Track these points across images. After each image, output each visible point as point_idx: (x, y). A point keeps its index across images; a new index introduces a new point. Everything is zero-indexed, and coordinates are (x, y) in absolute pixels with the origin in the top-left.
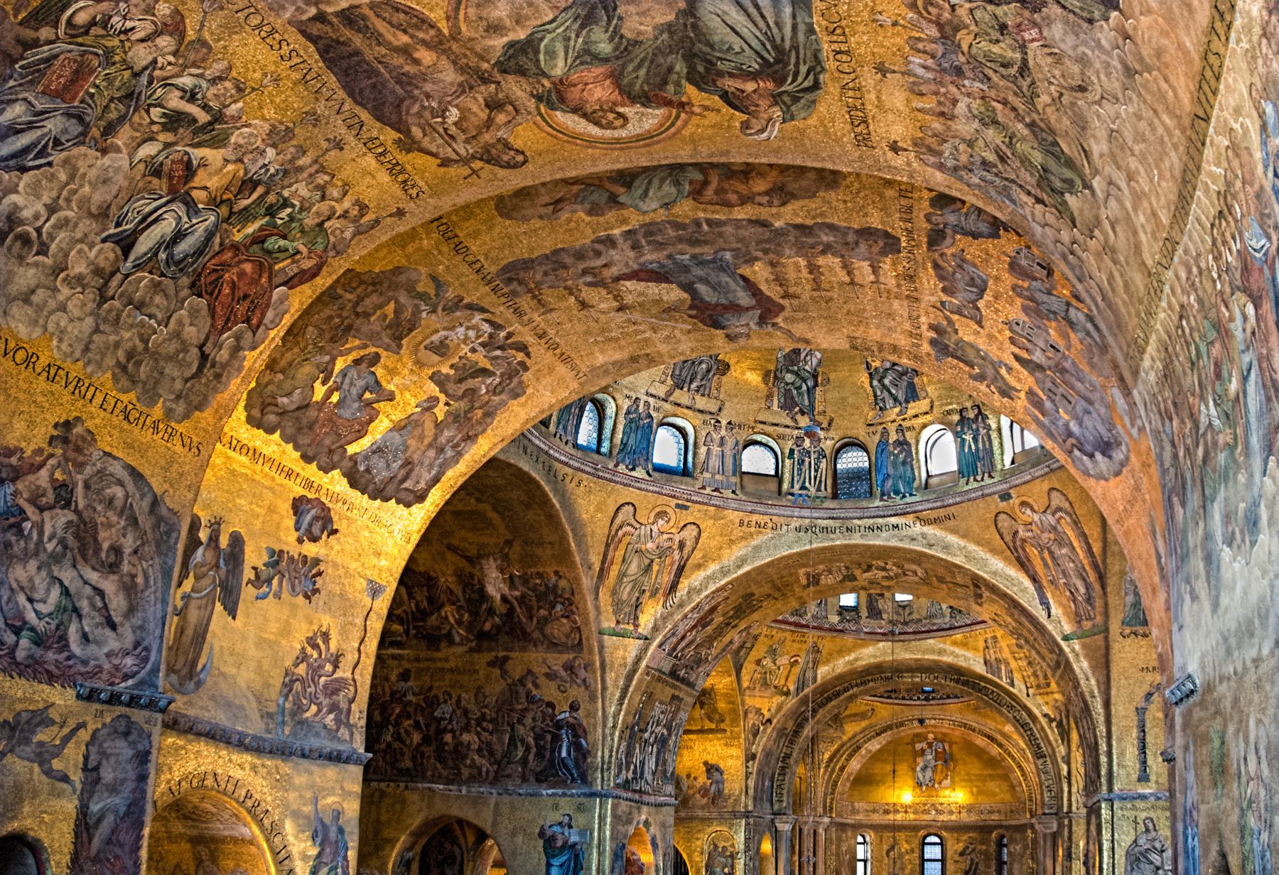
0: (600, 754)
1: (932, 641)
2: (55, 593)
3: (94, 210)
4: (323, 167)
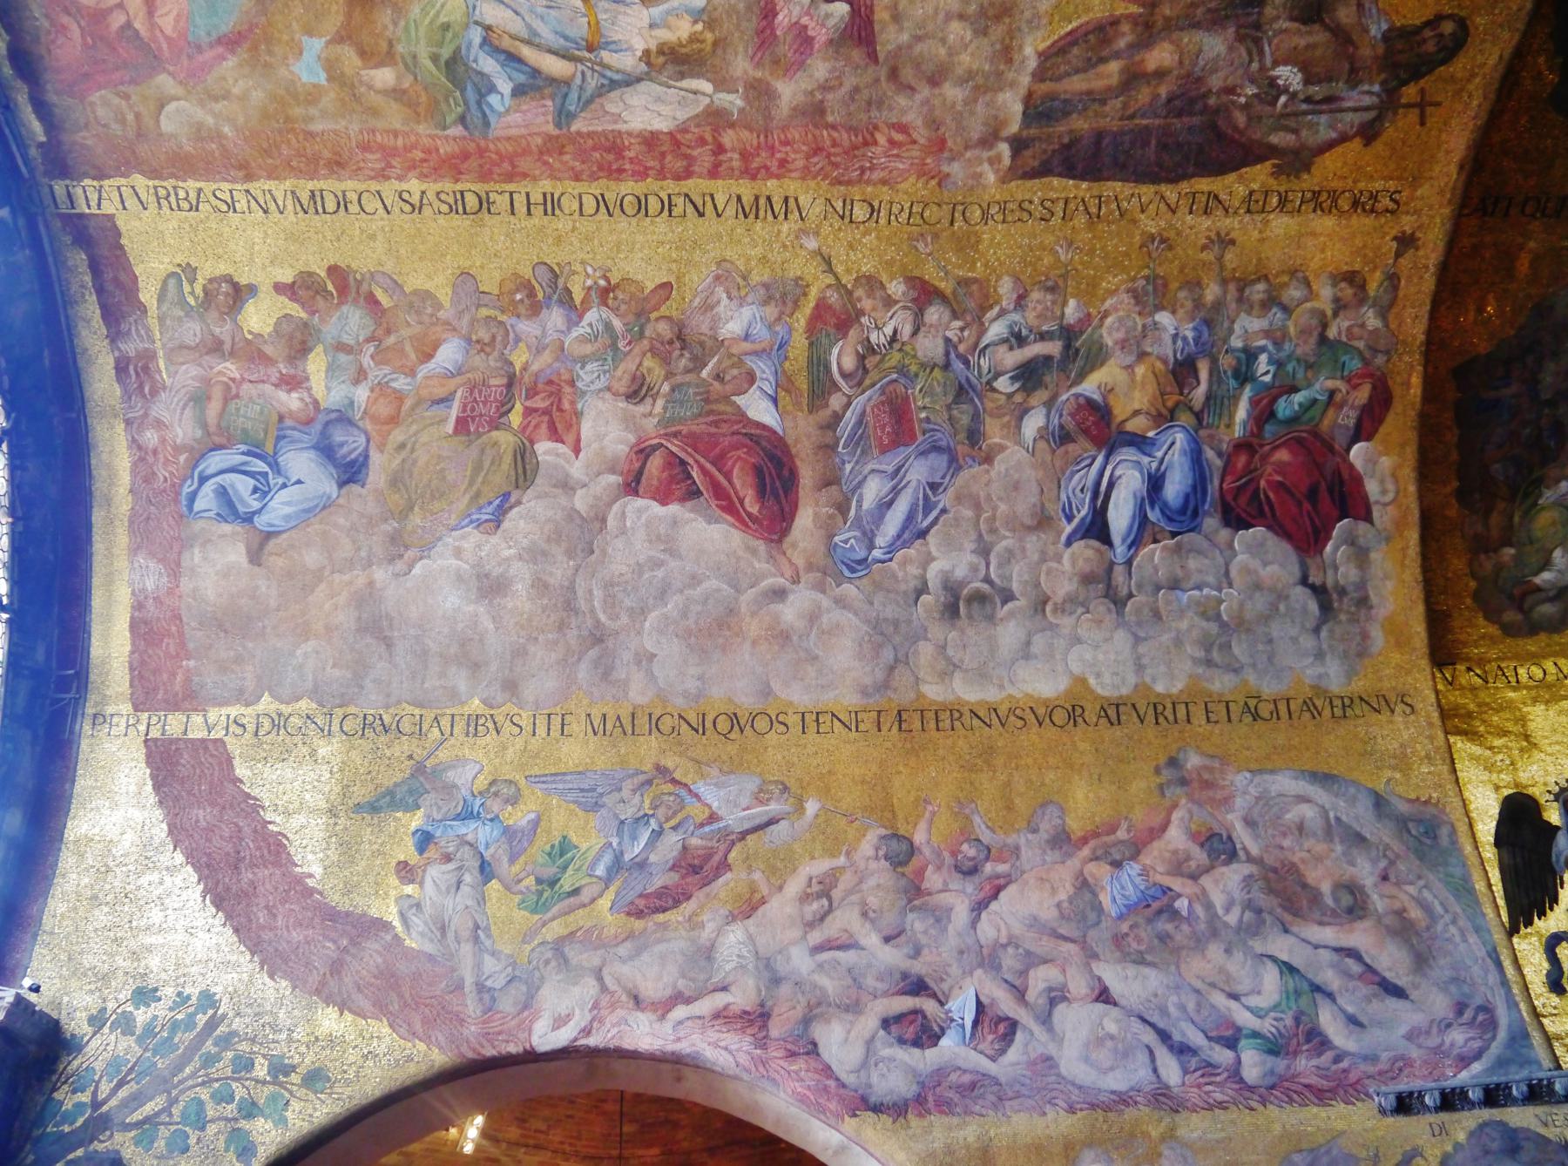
2: (1271, 978)
3: (1028, 521)
4: (1239, 280)
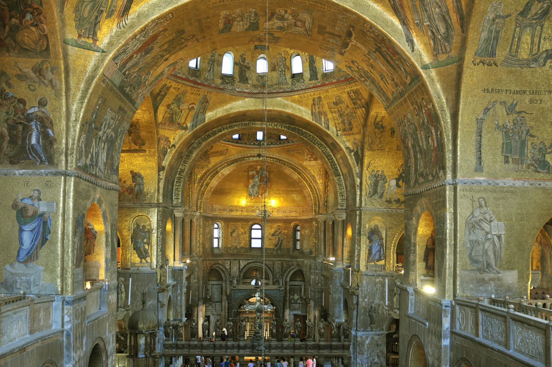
0: (64, 141)
1: (279, 99)
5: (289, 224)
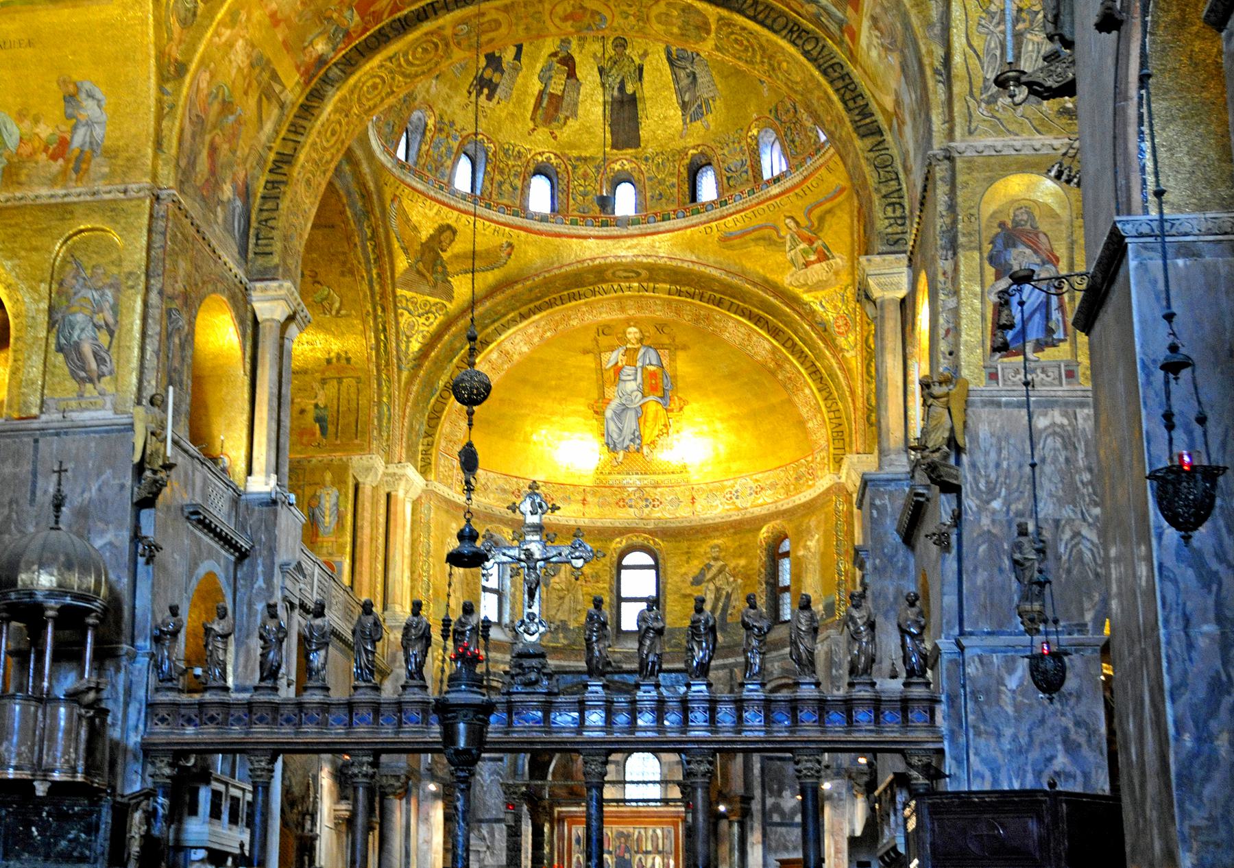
5: (750, 535)
